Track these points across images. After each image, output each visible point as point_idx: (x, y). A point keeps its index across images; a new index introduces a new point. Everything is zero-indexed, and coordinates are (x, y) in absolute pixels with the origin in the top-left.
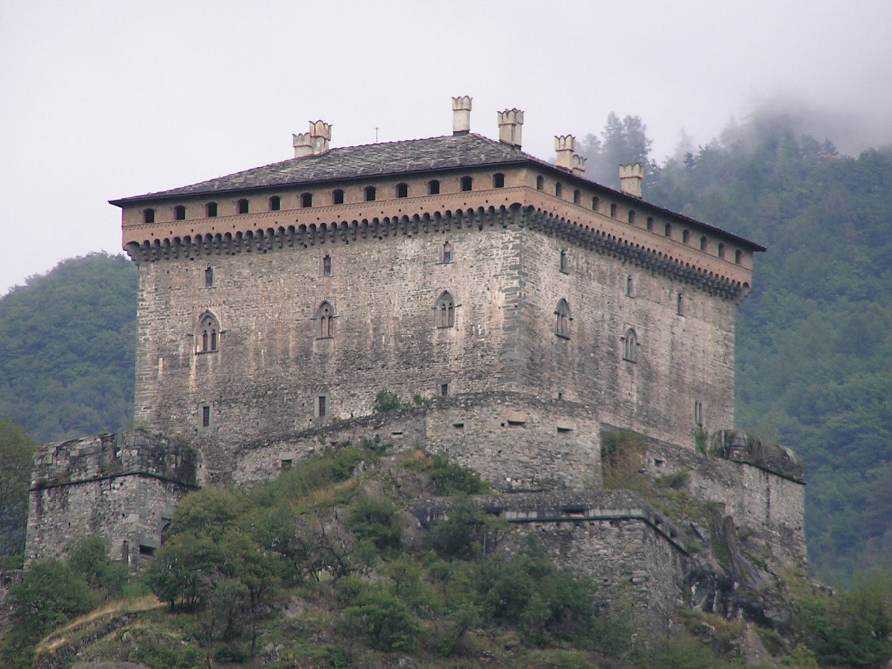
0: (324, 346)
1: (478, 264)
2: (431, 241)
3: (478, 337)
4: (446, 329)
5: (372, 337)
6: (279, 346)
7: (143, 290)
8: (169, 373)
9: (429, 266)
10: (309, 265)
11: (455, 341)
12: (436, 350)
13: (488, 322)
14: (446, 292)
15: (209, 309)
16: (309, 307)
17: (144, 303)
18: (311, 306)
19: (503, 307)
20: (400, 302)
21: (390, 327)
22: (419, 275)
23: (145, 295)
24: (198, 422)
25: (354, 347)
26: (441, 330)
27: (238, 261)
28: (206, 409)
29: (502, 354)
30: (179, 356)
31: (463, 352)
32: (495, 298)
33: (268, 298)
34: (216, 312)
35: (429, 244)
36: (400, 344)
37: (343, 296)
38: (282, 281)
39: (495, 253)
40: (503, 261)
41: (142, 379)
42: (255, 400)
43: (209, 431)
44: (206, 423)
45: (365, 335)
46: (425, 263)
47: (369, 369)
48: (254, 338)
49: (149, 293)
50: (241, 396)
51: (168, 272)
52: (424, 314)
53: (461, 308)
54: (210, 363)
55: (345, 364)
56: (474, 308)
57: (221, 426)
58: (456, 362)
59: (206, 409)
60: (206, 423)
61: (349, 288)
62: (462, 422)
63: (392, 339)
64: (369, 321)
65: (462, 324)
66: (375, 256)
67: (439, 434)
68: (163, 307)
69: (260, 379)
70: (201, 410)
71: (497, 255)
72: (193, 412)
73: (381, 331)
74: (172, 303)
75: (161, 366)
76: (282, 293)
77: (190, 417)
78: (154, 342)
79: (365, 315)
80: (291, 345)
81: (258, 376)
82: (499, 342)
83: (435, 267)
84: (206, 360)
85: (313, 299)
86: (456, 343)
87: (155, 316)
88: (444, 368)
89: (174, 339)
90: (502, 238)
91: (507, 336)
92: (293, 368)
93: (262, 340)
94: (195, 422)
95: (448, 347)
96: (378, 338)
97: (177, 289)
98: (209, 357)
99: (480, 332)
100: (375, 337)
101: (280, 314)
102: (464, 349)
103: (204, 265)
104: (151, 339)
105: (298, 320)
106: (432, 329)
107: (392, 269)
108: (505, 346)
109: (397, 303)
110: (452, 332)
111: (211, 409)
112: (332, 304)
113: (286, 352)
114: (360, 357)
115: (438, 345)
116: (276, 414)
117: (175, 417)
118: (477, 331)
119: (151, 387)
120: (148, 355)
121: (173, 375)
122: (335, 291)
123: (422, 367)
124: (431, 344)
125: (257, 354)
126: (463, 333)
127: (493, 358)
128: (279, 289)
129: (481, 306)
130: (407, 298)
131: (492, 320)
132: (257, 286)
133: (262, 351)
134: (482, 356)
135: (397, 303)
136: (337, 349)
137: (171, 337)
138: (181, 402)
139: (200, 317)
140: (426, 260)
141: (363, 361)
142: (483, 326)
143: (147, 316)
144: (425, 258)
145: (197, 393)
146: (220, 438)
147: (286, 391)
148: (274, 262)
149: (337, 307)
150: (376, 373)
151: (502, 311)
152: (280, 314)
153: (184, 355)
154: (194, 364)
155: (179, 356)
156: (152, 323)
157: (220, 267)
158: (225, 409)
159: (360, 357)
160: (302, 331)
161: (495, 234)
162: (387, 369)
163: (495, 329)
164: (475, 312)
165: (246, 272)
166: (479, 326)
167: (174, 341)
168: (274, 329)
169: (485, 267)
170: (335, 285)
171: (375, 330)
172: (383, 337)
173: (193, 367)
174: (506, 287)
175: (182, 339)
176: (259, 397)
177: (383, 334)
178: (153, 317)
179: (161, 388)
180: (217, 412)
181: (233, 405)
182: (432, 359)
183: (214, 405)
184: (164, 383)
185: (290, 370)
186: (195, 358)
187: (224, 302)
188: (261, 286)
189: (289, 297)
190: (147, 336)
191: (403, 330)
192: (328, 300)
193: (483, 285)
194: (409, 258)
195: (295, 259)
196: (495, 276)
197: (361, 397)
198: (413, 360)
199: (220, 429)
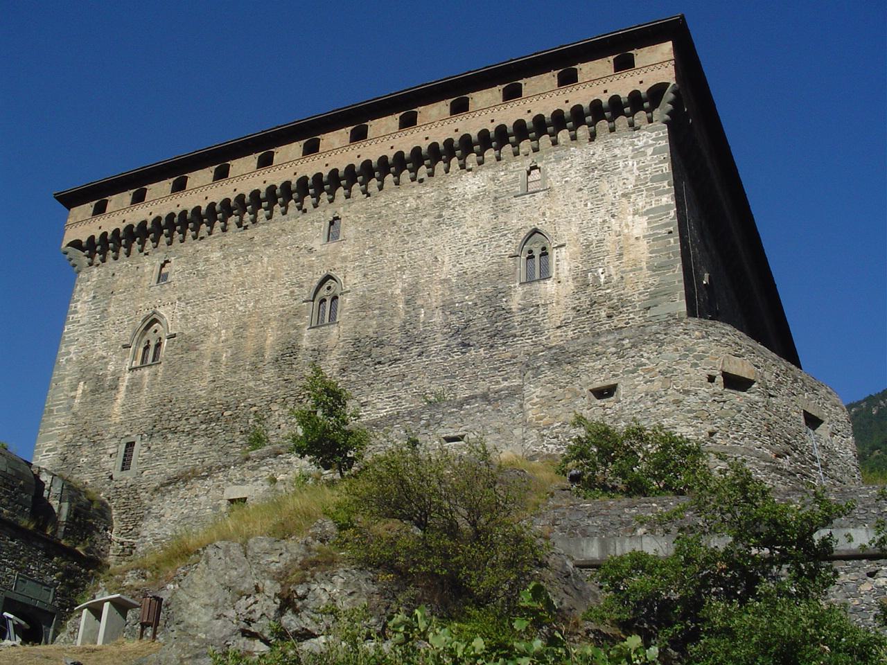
0: (321, 337)
1: (591, 184)
2: (506, 169)
3: (598, 287)
4: (537, 284)
5: (402, 313)
6: (250, 345)
7: (79, 300)
8: (89, 400)
9: (504, 201)
10: (310, 231)
11: (555, 300)
12: (518, 318)
13: (617, 263)
14: (535, 231)
15: (158, 309)
16: (302, 286)
17: (76, 316)
18: (305, 284)
19: (645, 237)
20: (453, 257)
21: (435, 296)
22: (486, 216)
23: (79, 307)
24: (114, 465)
25: (370, 332)
26: (527, 287)
27: (207, 246)
29: (649, 308)
31: (572, 314)
32: (627, 225)
33: (243, 284)
34: (166, 312)
35: (503, 173)
36: (454, 317)
37: (357, 264)
38: (266, 259)
39: (621, 164)
40: (637, 173)
41: (53, 410)
42: (204, 426)
43: (129, 476)
44: (125, 466)
45: (391, 312)
46: (496, 198)
47: (396, 360)
49: (85, 302)
50: (184, 422)
51: (114, 274)
52: (495, 267)
53: (563, 249)
54: (146, 380)
55: (355, 358)
56: (588, 246)
57: (147, 468)
58: (559, 332)
59: (130, 445)
60: (125, 466)
61: (367, 253)
62: (612, 382)
63: (438, 312)
64: (398, 291)
65: (567, 273)
66: (412, 203)
67: (557, 412)
68: (98, 316)
69: (217, 394)
70: (122, 448)
71: (626, 166)
72: (111, 451)
73: (419, 302)
74: (111, 310)
75: (80, 391)
76: (263, 275)
77: (106, 458)
78: (79, 362)
79: (391, 284)
80: (268, 342)
81: (213, 391)
82: (642, 290)
83: (514, 200)
84: (142, 377)
85: (310, 275)
86: (558, 303)
87: (85, 329)
88: (535, 344)
89: (105, 354)
90: (632, 144)
91: (658, 279)
92: (270, 373)
93: (227, 340)
94: (111, 465)
95: (542, 310)
96: (412, 313)
97: (121, 293)
98: (146, 371)
99: (602, 280)
100: (407, 312)
101: (257, 301)
102: (574, 308)
103: (160, 258)
104: (74, 359)
105: (283, 306)
106: (510, 288)
107: (440, 216)
108: (653, 295)
109: (447, 259)
110: (550, 287)
112: (340, 277)
113: (259, 352)
114: (380, 344)
115: (521, 310)
116: (233, 444)
118: (597, 278)
119: (61, 421)
120: (66, 381)
121: (93, 402)
122: (344, 259)
123: (492, 346)
124: (509, 311)
125: (216, 361)
126: (571, 286)
127: (632, 316)
128: (259, 271)
129: (600, 241)
130: (464, 251)
131: (625, 259)
132: (228, 272)
133: (224, 355)
134: (609, 317)
135: (447, 259)
136: (342, 339)
137: (100, 352)
138: (96, 438)
139: (144, 321)
140: (497, 195)
141: (387, 350)
142: (607, 270)
143: (76, 331)
144: (496, 191)
147: (255, 409)
148: (256, 238)
149: (347, 279)
150: (407, 366)
151: (643, 244)
152: (257, 301)
153: (113, 374)
154: (126, 384)
156: (81, 339)
157: (181, 257)
158: (157, 443)
159: (380, 344)
160: (288, 320)
161: (620, 141)
162: (428, 357)
163: (631, 271)
164: (590, 253)
165: (216, 256)
166: (600, 270)
167: (104, 358)
168: (245, 323)
169: (605, 187)
170: (346, 250)
171: (407, 302)
172: (423, 311)
173: (123, 389)
174: (648, 207)
175: (115, 353)
176: (211, 421)
177: (422, 307)
178: (84, 330)
179: (74, 422)
180: (145, 449)
181: (170, 436)
182: (513, 331)
184: (79, 413)
185: (264, 377)
186: (128, 376)
187: (179, 299)
188: (234, 271)
189: (273, 277)
190: (71, 356)
191: (458, 296)
192: (333, 273)
193: (603, 211)
194: (470, 197)
195: (288, 228)
196: (624, 195)
197: (380, 406)
198: (475, 337)
199: (145, 473)
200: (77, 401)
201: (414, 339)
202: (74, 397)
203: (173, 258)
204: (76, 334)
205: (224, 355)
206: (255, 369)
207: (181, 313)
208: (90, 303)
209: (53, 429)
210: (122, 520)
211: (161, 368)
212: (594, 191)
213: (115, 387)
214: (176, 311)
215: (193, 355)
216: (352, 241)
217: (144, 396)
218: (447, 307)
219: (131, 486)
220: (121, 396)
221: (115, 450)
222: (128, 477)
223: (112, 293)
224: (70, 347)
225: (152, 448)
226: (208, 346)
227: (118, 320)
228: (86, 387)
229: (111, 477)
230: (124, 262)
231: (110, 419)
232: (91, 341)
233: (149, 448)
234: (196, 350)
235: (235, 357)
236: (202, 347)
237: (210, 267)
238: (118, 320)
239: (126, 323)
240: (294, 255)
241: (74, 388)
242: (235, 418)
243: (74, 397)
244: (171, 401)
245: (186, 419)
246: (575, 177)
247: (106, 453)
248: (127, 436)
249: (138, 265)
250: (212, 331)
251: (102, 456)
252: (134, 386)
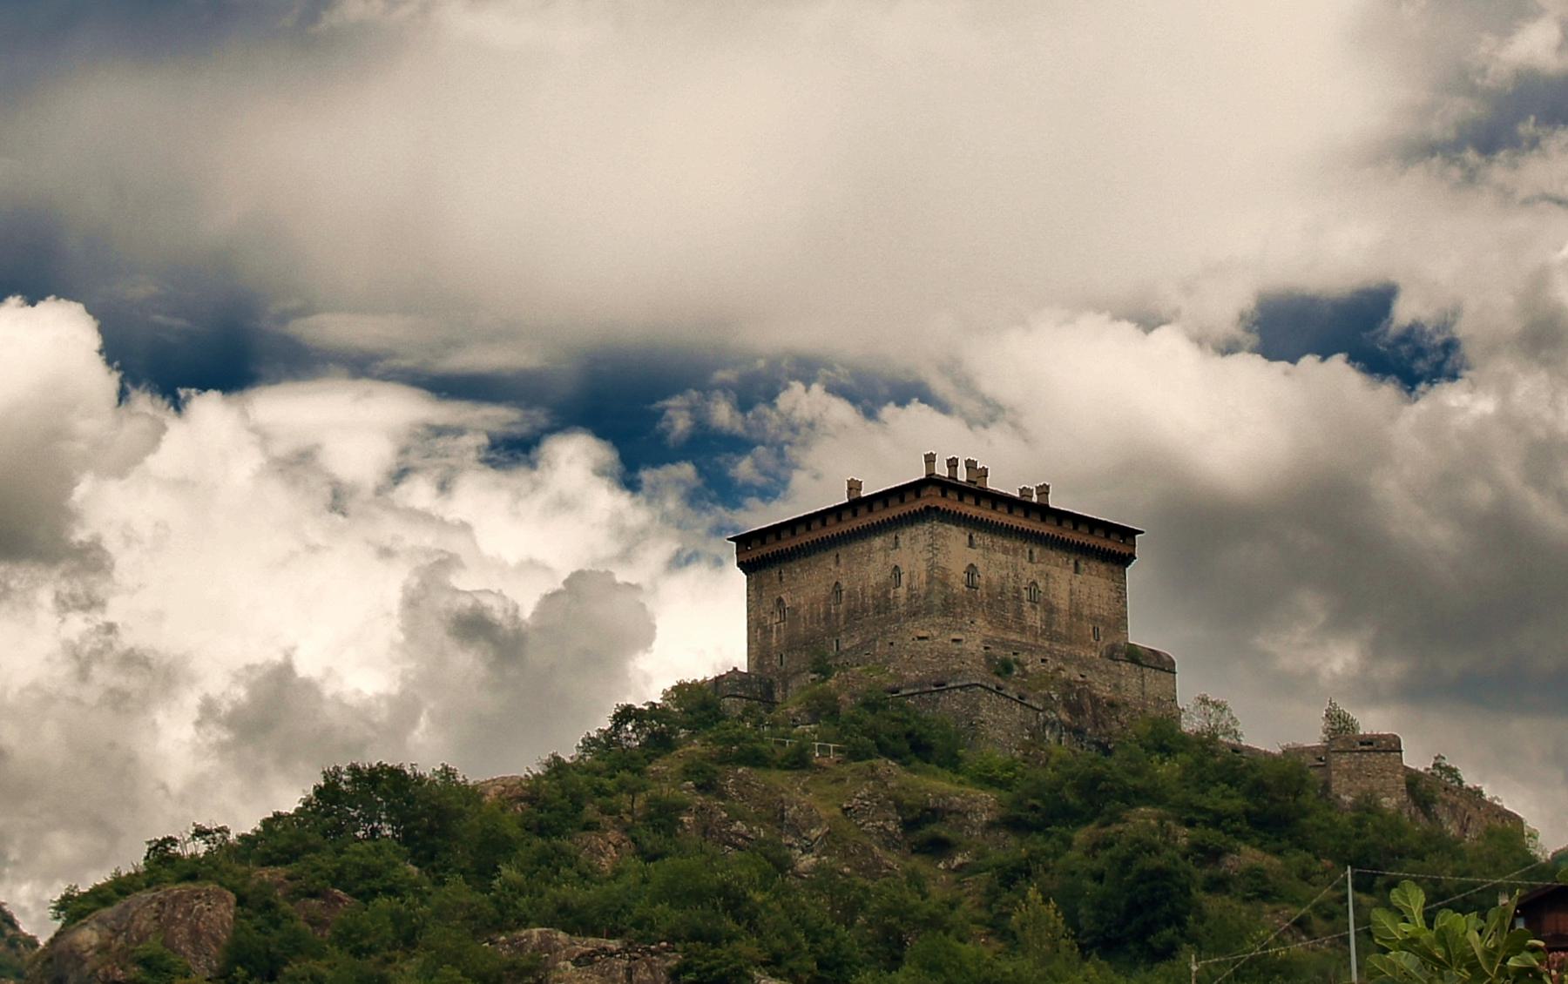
6: (815, 612)
21: (869, 591)
22: (883, 558)
24: (777, 664)
28: (781, 656)
43: (783, 669)
54: (782, 628)
59: (781, 656)
70: (779, 657)
75: (758, 633)
78: (756, 620)
92: (823, 624)
98: (782, 624)
110: (900, 590)
125: (805, 618)
142: (915, 584)
158: (790, 654)
171: (862, 594)
173: (774, 630)
186: (775, 626)
201: (865, 610)
206: (818, 622)
211: (787, 623)
212: (912, 549)
213: (772, 631)
215: (797, 617)
217: (783, 635)
218: (873, 597)
220: (774, 635)
226: (801, 612)
230: (765, 571)
235: (811, 617)
236: (800, 613)
241: (756, 632)
246: (907, 543)
252: (779, 630)
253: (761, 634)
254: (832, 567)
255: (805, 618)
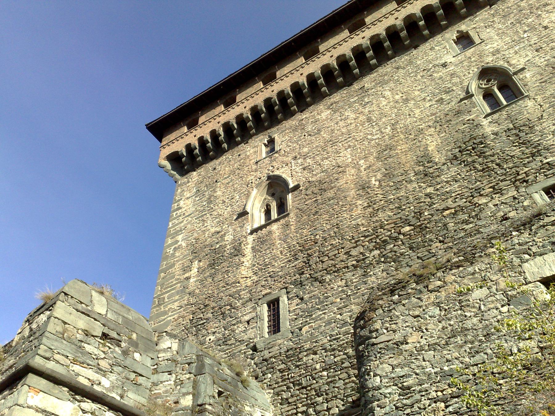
17: (180, 211)
28: (274, 305)
30: (225, 246)
33: (369, 120)
44: (275, 327)
48: (353, 171)
49: (188, 198)
59: (274, 305)
60: (275, 327)
72: (247, 318)
75: (195, 271)
77: (240, 328)
81: (372, 215)
87: (191, 218)
89: (218, 229)
94: (251, 333)
98: (275, 227)
111: (284, 300)
117: (212, 338)
120: (177, 266)
125: (364, 187)
137: (213, 230)
145: (256, 283)
146: (307, 346)
154: (250, 246)
155: (225, 246)
165: (326, 114)
167: (218, 233)
173: (248, 250)
175: (231, 224)
181: (328, 278)
183: (288, 293)
186: (250, 238)
189: (406, 101)
190: (179, 244)
199: (304, 330)
200: (192, 280)
202: (188, 278)
203: (276, 135)
204: (182, 224)
205: (373, 179)
207: (301, 167)
208: (194, 197)
209: (166, 317)
210: (285, 401)
213: (238, 251)
214: (293, 168)
216: (496, 37)
219: (288, 351)
221: (254, 314)
222: (279, 342)
223: (216, 181)
224: (177, 237)
225: (306, 297)
227: (228, 198)
228: (201, 264)
229: (255, 349)
231: (238, 284)
232: (201, 224)
233: (302, 299)
234: (332, 188)
237: (322, 124)
238: (228, 198)
239: (238, 197)
240: (422, 77)
241: (186, 269)
242: (422, 229)
243: (188, 278)
244: (317, 243)
245: (347, 253)
247: (241, 322)
248: (266, 294)
249: (239, 154)
250: (347, 166)
251: (236, 327)
253: (201, 271)
254: (449, 59)
255: (364, 187)
